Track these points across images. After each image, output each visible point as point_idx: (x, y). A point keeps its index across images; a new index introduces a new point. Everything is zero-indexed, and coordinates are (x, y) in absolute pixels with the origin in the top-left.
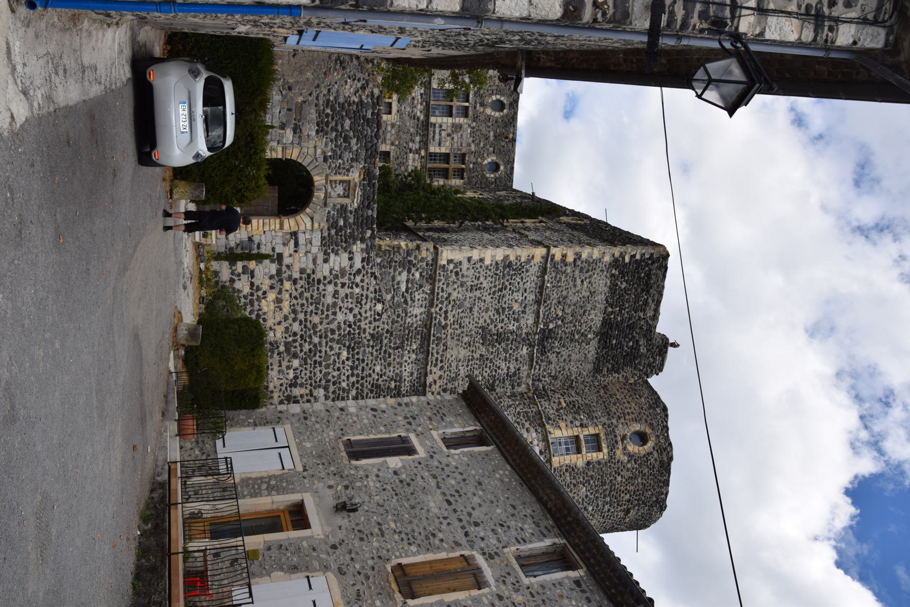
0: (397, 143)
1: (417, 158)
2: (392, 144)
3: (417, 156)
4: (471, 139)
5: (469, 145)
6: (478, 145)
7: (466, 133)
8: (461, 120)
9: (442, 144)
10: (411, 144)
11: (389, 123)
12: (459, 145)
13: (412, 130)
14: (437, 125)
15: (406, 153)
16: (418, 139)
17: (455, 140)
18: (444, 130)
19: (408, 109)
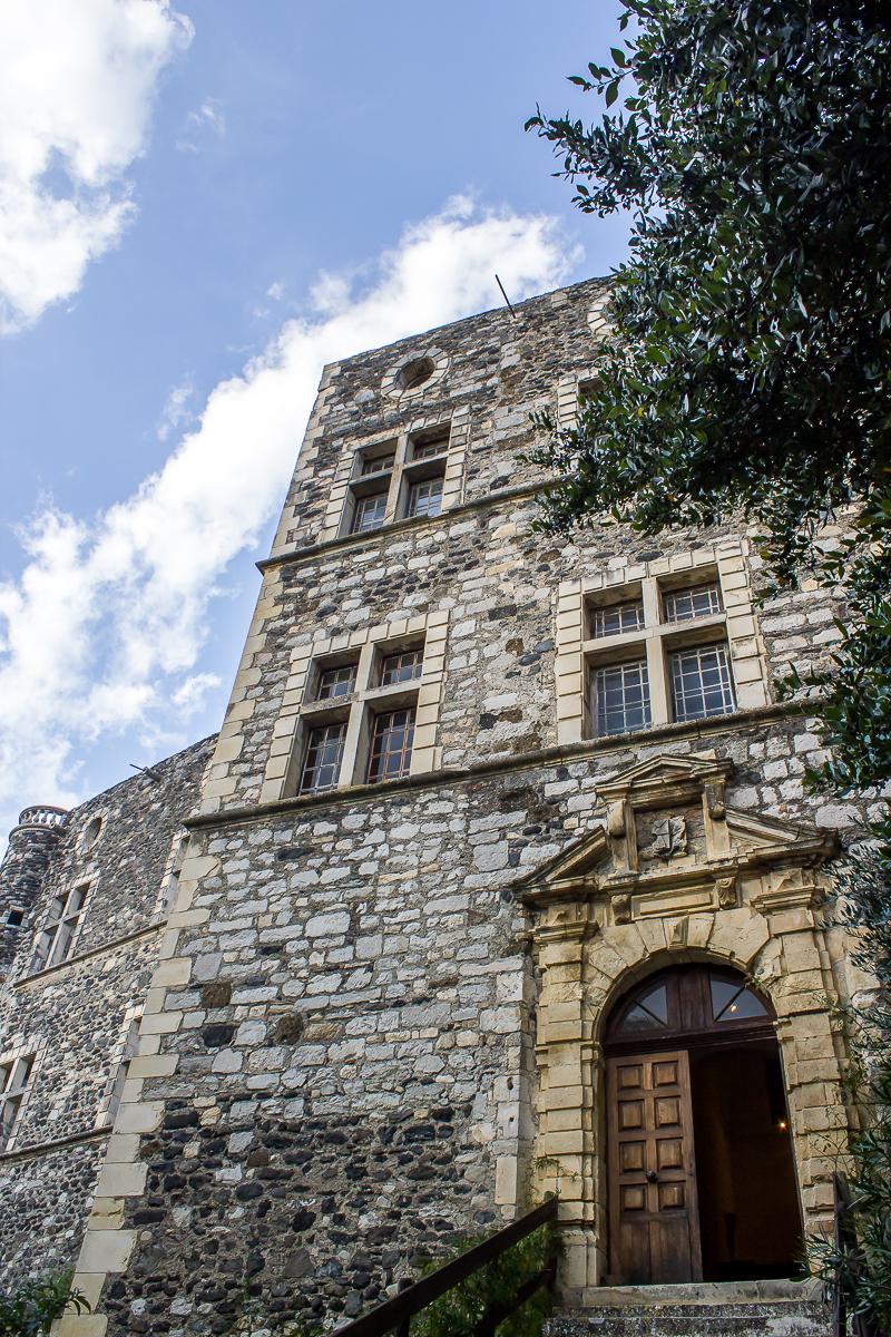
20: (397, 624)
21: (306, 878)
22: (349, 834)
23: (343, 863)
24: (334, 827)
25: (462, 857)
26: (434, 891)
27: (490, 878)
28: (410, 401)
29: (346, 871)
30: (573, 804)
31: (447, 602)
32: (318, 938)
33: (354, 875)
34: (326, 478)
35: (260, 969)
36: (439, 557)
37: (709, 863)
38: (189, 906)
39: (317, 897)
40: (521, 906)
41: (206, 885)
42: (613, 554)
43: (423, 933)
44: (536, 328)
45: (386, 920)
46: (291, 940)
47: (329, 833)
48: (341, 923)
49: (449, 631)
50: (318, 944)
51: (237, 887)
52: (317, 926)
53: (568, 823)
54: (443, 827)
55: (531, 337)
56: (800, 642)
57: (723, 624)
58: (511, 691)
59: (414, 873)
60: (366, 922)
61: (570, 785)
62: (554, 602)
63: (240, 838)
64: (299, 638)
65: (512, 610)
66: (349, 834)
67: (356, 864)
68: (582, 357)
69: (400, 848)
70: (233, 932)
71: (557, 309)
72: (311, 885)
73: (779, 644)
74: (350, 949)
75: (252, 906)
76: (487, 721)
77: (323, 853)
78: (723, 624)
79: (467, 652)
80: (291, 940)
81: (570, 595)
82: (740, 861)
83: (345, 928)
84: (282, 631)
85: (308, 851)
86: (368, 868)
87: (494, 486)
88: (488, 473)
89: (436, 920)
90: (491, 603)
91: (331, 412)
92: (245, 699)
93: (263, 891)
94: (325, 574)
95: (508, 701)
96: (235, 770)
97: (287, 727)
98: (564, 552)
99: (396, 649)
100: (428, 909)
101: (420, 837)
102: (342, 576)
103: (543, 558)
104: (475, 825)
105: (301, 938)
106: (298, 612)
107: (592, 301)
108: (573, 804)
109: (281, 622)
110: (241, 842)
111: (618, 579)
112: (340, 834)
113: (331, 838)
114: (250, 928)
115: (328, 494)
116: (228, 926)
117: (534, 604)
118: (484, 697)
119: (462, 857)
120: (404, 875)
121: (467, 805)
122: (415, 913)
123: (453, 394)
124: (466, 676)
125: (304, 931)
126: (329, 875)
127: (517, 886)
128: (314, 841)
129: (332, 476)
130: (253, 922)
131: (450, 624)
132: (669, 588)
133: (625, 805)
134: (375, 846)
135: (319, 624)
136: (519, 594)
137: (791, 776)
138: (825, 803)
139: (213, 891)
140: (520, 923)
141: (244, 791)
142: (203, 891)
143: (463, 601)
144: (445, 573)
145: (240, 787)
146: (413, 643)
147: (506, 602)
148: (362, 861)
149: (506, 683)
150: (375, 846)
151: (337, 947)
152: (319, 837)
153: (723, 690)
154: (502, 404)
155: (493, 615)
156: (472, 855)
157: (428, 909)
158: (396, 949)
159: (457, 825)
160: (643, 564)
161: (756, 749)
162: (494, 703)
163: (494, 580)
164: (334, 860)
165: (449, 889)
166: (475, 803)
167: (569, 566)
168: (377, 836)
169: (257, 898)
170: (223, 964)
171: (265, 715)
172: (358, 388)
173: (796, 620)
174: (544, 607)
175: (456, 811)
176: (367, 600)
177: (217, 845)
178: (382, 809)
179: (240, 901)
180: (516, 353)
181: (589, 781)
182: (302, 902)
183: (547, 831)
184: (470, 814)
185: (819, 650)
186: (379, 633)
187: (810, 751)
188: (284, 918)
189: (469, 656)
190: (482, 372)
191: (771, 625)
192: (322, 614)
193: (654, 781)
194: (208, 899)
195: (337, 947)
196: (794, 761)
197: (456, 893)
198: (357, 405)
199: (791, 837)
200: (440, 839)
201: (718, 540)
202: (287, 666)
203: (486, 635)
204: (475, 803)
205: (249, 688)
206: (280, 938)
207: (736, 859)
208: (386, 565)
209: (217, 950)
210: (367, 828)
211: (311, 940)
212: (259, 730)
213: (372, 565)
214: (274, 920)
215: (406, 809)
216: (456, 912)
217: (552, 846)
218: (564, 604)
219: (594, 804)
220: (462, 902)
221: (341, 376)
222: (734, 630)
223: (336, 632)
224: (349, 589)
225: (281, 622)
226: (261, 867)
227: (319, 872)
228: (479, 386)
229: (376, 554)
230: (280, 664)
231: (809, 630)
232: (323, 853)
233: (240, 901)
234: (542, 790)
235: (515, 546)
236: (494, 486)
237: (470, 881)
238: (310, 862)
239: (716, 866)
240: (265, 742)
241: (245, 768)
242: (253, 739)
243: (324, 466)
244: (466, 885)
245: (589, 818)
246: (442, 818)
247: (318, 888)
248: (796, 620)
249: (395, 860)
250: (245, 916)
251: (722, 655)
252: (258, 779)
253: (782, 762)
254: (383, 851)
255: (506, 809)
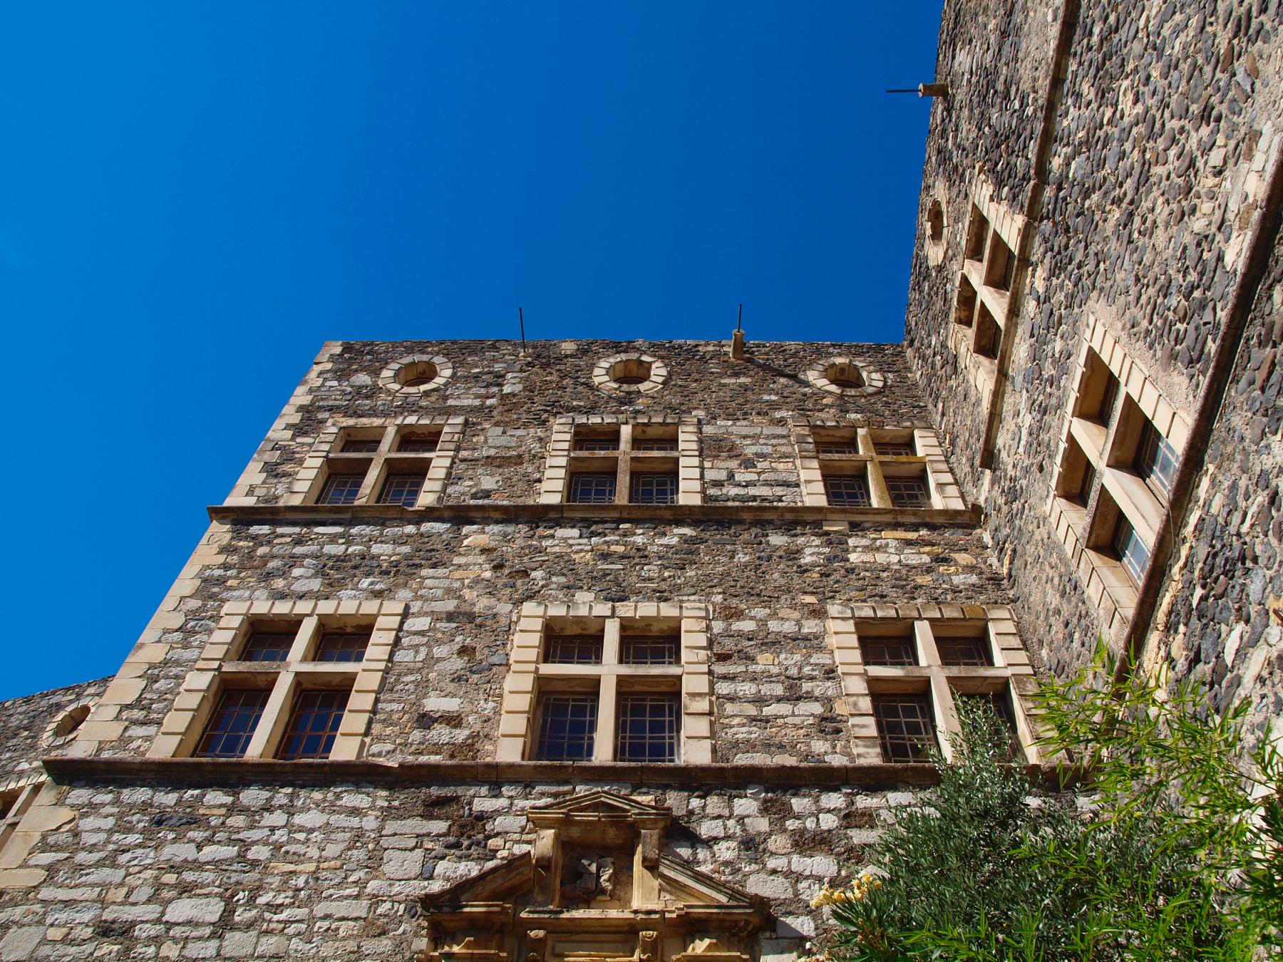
0: (809, 599)
1: (864, 542)
2: (818, 613)
3: (852, 542)
4: (757, 419)
5: (781, 422)
6: (774, 406)
7: (734, 429)
8: (687, 439)
9: (793, 479)
10: (807, 559)
11: (718, 626)
12: (784, 441)
13: (742, 558)
14: (712, 491)
15: (850, 571)
16: (777, 539)
17: (769, 450)
18: (731, 476)
19: (651, 570)
20: (348, 604)
21: (184, 851)
22: (244, 810)
23: (230, 842)
24: (228, 800)
25: (369, 859)
26: (332, 891)
27: (397, 888)
28: (406, 398)
29: (232, 851)
30: (500, 823)
31: (404, 594)
32: (178, 924)
33: (241, 857)
34: (303, 444)
35: (92, 954)
36: (406, 549)
37: (636, 912)
38: (20, 862)
39: (189, 876)
40: (426, 924)
41: (51, 840)
42: (582, 588)
43: (307, 937)
44: (544, 366)
45: (267, 915)
46: (142, 922)
47: (221, 806)
48: (212, 910)
49: (402, 623)
50: (175, 932)
51: (92, 848)
52: (181, 910)
53: (492, 843)
54: (355, 822)
55: (537, 374)
56: (751, 710)
57: (679, 678)
58: (454, 696)
59: (311, 867)
60: (240, 916)
61: (502, 803)
62: (514, 619)
63: (110, 792)
64: (236, 593)
65: (471, 617)
66: (244, 810)
67: (246, 845)
68: (582, 404)
69: (301, 836)
70: (68, 904)
71: (566, 356)
72: (186, 860)
73: (730, 708)
74: (214, 944)
75: (105, 874)
76: (425, 720)
77: (209, 827)
78: (679, 678)
79: (416, 648)
80: (142, 922)
81: (531, 618)
82: (667, 915)
83: (215, 918)
84: (221, 581)
85: (194, 821)
86: (259, 853)
87: (474, 496)
88: (471, 483)
89: (326, 924)
90: (450, 605)
91: (323, 385)
92: (159, 641)
93: (123, 858)
94: (282, 536)
95: (451, 705)
96: (125, 715)
97: (200, 681)
98: (534, 574)
99: (340, 628)
100: (320, 909)
101: (327, 829)
102: (299, 542)
103: (510, 575)
104: (391, 826)
105: (158, 921)
106: (242, 568)
107: (599, 358)
108: (500, 823)
109: (221, 572)
110: (109, 797)
111: (583, 611)
112: (231, 810)
113: (223, 811)
114: (94, 901)
115: (301, 462)
116: (63, 894)
117: (495, 616)
118: (425, 696)
119: (369, 859)
120: (300, 868)
121: (386, 804)
122: (302, 912)
123: (451, 402)
124: (411, 671)
125: (163, 914)
126: (209, 852)
127: (429, 901)
128: (201, 811)
129: (311, 445)
130: (99, 895)
131: (406, 614)
132: (629, 633)
133: (557, 837)
134: (273, 829)
135: (263, 584)
136: (482, 604)
137: (727, 838)
138: (758, 872)
139: (57, 848)
140: (422, 943)
141: (131, 739)
142: (44, 846)
143: (422, 596)
144: (408, 566)
145: (127, 734)
146: (359, 627)
147: (465, 608)
148: (255, 843)
149: (451, 687)
150: (273, 829)
151: (200, 938)
152: (209, 807)
153: (667, 741)
154: (497, 424)
155: (450, 617)
156: (382, 859)
157: (320, 909)
158: (272, 951)
159: (370, 823)
160: (610, 604)
161: (695, 803)
162: (434, 703)
163: (457, 585)
164: (220, 836)
165: (347, 892)
166: (396, 803)
167: (536, 588)
168: (278, 818)
169: (114, 865)
170: (44, 941)
171: (178, 663)
172: (356, 371)
173: (748, 689)
174: (504, 621)
175: (372, 808)
176: (320, 572)
177: (80, 795)
178: (290, 790)
179: (90, 867)
180: (519, 383)
181: (520, 803)
182: (170, 878)
183: (469, 847)
184: (388, 813)
185: (768, 721)
186: (326, 607)
187: (748, 816)
188: (143, 893)
189: (417, 652)
190: (483, 391)
191: (723, 688)
192: (269, 576)
193: (591, 816)
194: (47, 858)
195: (200, 938)
196: (731, 823)
197: (357, 897)
198: (352, 387)
199: (723, 899)
200: (348, 835)
201: (685, 598)
202: (216, 618)
203: (439, 635)
204: (396, 803)
205: (166, 631)
206: (130, 918)
207: (663, 912)
208: (349, 543)
209: (41, 922)
210: (268, 808)
211: (170, 925)
212: (167, 677)
213: (333, 539)
214: (128, 895)
215: (317, 795)
216: (351, 919)
217: (471, 864)
218: (523, 624)
219: (523, 829)
220: (360, 909)
221: (341, 355)
222: (688, 685)
223: (282, 596)
224: (305, 556)
225: (221, 572)
226: (130, 830)
227: (199, 847)
228: (477, 402)
229: (339, 529)
230: (209, 613)
231: (760, 701)
232: (209, 827)
233: (90, 867)
234: (470, 803)
235: (484, 557)
236: (474, 496)
237: (373, 886)
238: (190, 834)
239: (640, 916)
240: (170, 691)
241: (137, 714)
242: (156, 686)
243: (305, 434)
244: (368, 890)
245: (518, 842)
246: (355, 812)
247: (197, 866)
248: (748, 689)
249: (292, 848)
250: (93, 885)
251: (671, 707)
252: (152, 730)
253: (720, 822)
254: (280, 835)
255: (428, 816)
